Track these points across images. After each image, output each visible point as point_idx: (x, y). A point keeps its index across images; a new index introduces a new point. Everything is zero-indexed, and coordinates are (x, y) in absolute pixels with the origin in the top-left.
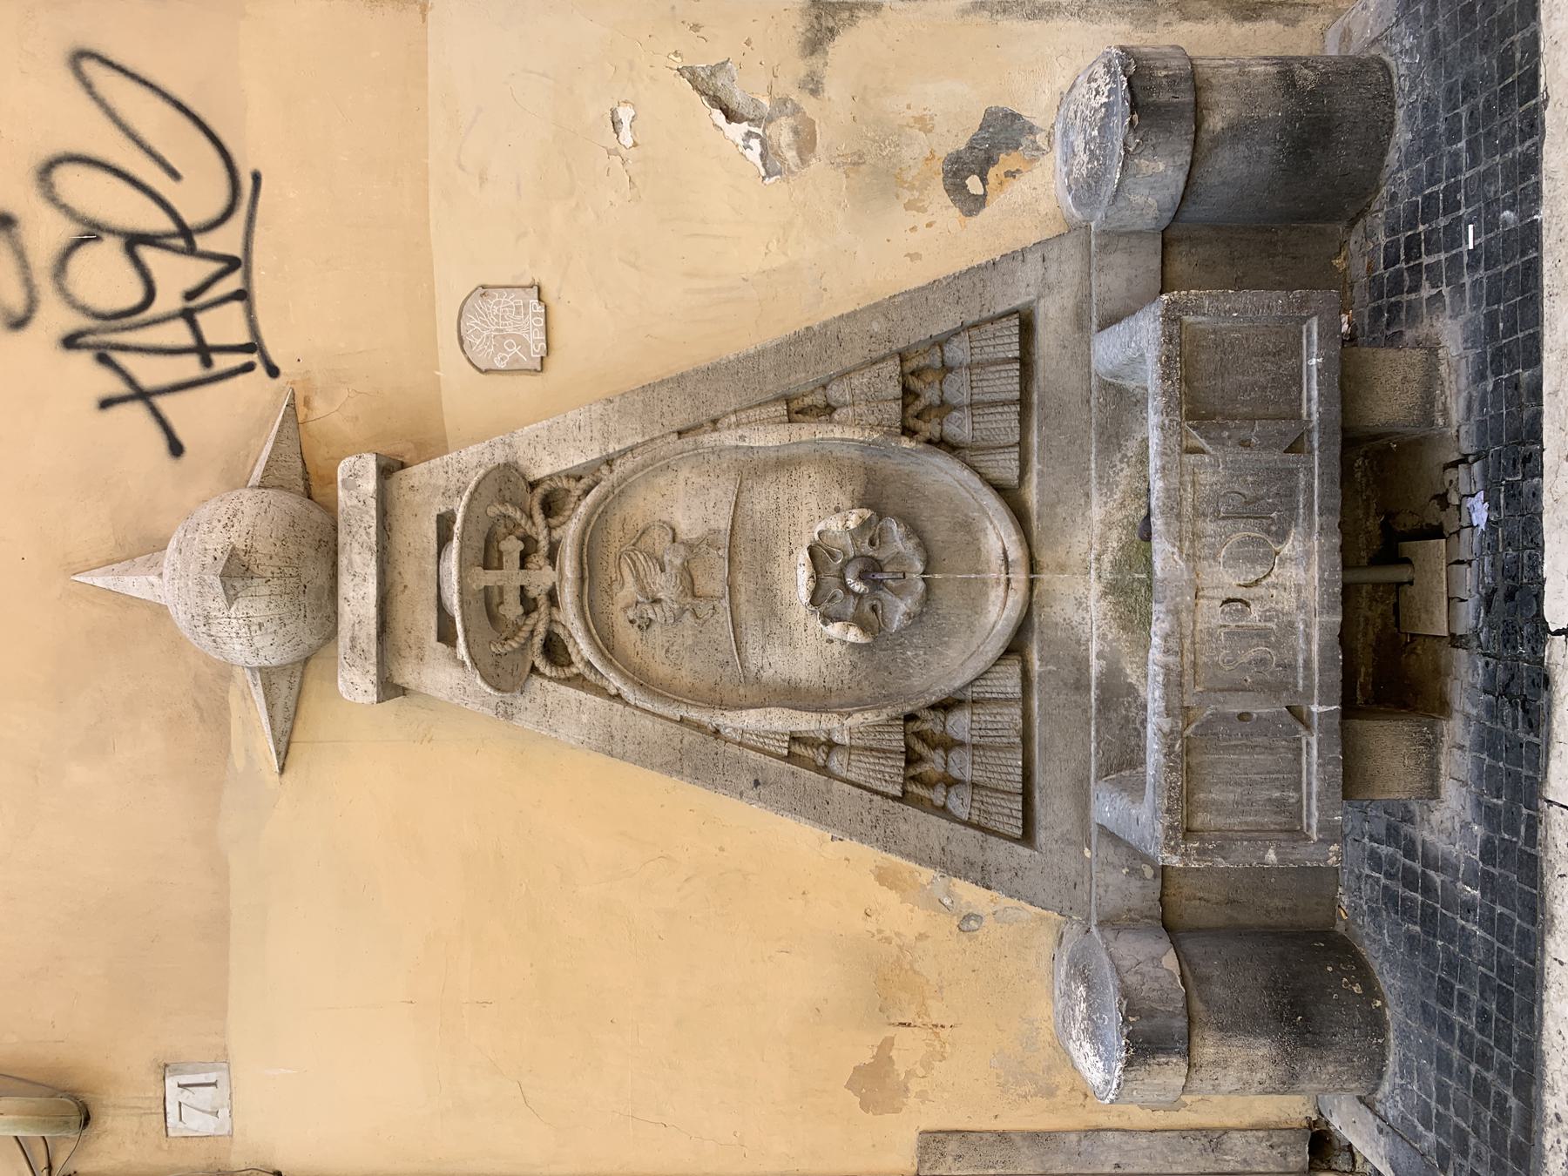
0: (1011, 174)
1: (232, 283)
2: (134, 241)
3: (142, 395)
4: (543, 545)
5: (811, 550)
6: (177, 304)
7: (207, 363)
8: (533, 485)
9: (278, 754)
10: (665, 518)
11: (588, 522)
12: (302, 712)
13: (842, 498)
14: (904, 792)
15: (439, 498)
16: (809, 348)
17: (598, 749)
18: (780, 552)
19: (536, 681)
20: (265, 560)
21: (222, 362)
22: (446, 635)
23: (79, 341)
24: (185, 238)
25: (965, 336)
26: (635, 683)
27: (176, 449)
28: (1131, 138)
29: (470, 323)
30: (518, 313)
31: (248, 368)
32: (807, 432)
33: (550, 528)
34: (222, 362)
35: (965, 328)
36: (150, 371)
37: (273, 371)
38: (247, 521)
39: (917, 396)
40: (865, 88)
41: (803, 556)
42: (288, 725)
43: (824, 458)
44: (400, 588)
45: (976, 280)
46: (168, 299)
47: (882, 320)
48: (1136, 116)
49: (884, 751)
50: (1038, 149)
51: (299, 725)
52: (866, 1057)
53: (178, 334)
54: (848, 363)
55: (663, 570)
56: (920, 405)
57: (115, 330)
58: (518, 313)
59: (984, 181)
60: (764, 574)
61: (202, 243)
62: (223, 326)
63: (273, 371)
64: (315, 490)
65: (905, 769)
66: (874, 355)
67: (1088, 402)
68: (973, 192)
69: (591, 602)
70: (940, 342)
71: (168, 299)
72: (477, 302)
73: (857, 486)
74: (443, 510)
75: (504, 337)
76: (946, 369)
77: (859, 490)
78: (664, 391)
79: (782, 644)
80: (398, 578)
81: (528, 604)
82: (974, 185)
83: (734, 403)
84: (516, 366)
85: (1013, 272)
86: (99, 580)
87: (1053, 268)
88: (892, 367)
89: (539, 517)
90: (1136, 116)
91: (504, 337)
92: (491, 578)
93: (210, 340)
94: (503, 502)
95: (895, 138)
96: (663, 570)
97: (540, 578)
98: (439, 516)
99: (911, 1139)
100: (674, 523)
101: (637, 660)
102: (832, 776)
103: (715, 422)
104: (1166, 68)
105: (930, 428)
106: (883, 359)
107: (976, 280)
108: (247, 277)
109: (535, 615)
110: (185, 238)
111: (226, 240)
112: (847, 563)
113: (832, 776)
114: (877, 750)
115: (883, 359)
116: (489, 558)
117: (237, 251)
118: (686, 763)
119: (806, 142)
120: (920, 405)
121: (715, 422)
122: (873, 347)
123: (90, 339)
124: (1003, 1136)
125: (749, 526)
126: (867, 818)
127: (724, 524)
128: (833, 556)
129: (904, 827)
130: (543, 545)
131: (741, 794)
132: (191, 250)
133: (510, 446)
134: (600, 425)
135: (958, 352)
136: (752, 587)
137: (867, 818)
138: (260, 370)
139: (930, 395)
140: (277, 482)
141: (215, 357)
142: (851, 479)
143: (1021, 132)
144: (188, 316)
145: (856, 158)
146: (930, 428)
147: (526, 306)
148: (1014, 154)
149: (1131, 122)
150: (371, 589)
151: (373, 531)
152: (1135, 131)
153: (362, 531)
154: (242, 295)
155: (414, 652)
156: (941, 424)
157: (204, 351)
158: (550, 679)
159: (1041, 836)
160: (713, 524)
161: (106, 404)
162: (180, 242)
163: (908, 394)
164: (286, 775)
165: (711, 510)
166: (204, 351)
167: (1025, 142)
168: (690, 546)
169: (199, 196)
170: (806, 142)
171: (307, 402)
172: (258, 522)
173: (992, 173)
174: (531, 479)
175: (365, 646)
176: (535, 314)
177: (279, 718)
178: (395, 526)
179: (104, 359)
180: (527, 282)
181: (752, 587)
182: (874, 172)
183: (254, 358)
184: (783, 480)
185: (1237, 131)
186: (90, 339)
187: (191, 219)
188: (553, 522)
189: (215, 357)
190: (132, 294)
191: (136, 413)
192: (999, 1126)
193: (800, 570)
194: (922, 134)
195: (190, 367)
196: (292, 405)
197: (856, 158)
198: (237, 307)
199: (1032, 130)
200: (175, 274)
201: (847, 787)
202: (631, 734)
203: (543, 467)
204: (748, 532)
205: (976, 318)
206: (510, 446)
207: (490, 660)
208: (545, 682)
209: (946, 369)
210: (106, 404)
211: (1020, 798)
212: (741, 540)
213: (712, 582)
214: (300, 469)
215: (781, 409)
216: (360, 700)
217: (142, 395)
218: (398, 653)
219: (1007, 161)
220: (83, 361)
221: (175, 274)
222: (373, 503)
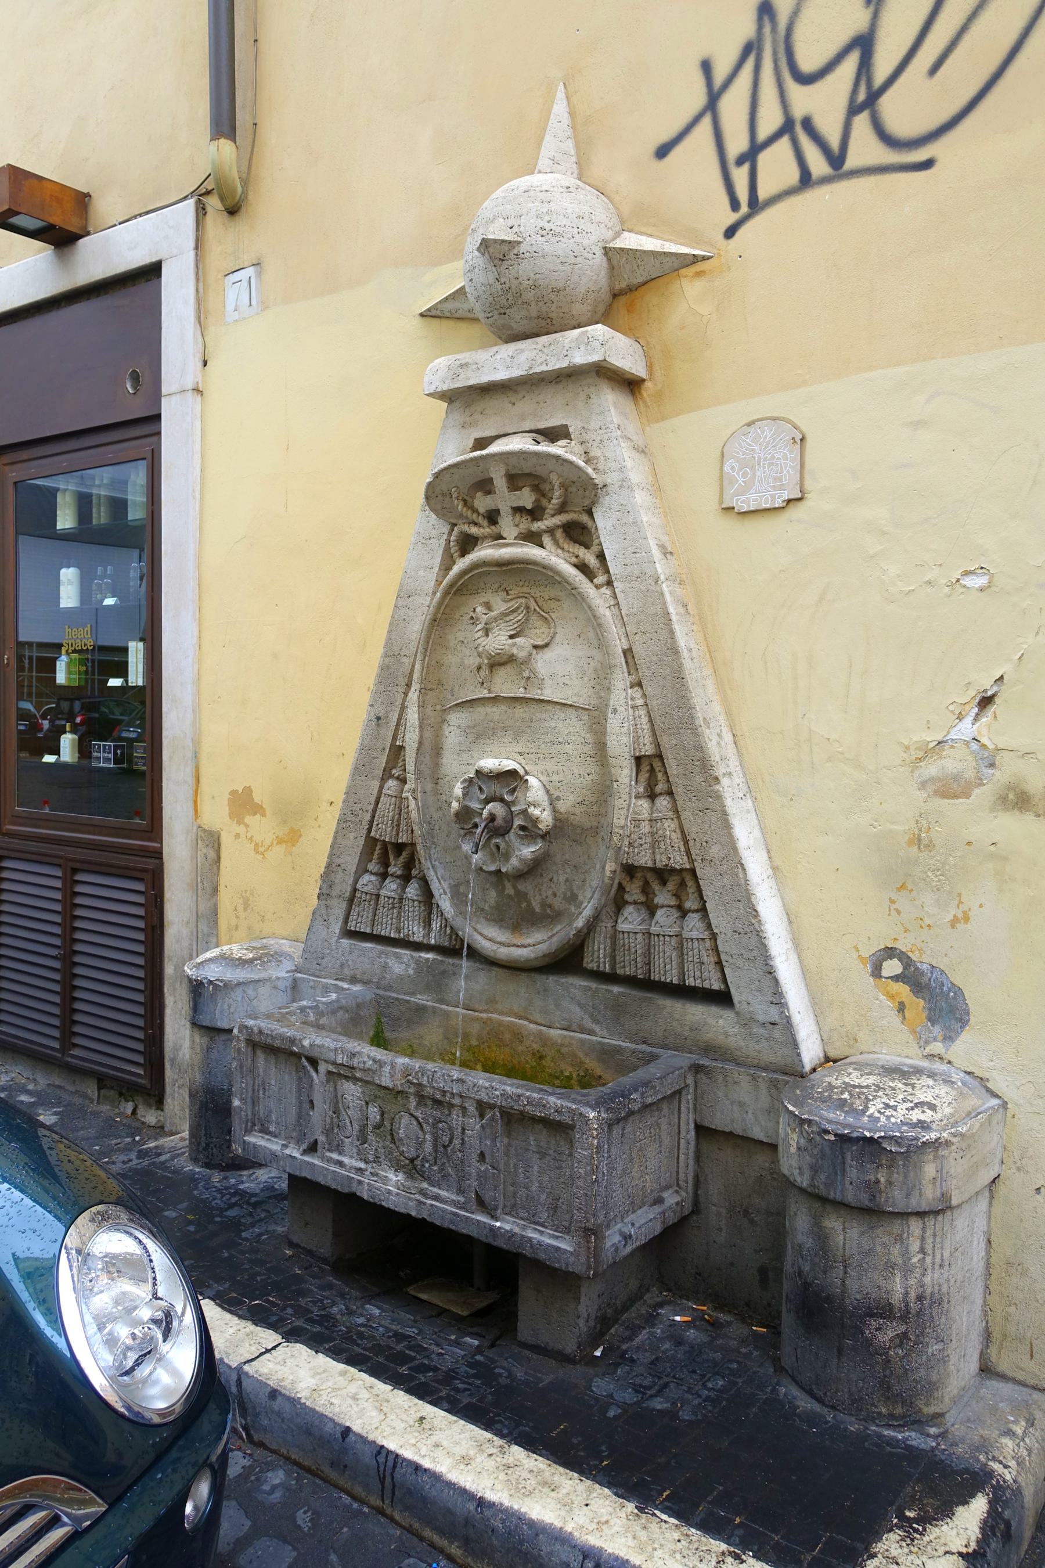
0: (901, 1008)
1: (818, 165)
2: (864, 44)
3: (713, 99)
4: (537, 526)
5: (512, 774)
6: (798, 113)
7: (740, 161)
8: (590, 513)
9: (429, 310)
10: (558, 638)
11: (544, 567)
12: (461, 325)
13: (569, 803)
14: (376, 840)
15: (580, 425)
16: (698, 779)
17: (401, 585)
18: (521, 744)
19: (446, 529)
20: (513, 272)
21: (740, 176)
22: (481, 443)
23: (766, 18)
24: (866, 101)
25: (706, 935)
26: (435, 614)
27: (663, 151)
28: (815, 1128)
29: (767, 431)
30: (775, 479)
31: (735, 205)
32: (624, 773)
33: (551, 531)
34: (740, 176)
35: (714, 937)
36: (734, 106)
37: (730, 232)
38: (549, 248)
39: (664, 883)
40: (1005, 859)
41: (509, 765)
42: (448, 315)
43: (604, 790)
44: (513, 399)
45: (755, 952)
46: (804, 100)
47: (721, 854)
48: (833, 1138)
49: (398, 826)
50: (927, 1042)
51: (451, 323)
52: (257, 798)
53: (770, 120)
54: (686, 816)
55: (511, 637)
56: (656, 886)
57: (775, 53)
58: (775, 479)
59: (896, 978)
60: (505, 729)
61: (862, 122)
62: (777, 167)
63: (730, 232)
64: (622, 300)
65: (390, 843)
66: (691, 843)
67: (645, 1043)
68: (885, 964)
69: (489, 573)
70: (703, 910)
71: (804, 100)
72: (788, 432)
73: (579, 816)
74: (571, 430)
75: (752, 468)
76: (683, 913)
77: (575, 820)
78: (664, 635)
79: (460, 743)
80: (520, 396)
81: (492, 516)
82: (892, 967)
83: (654, 703)
84: (725, 483)
85: (760, 990)
86: (560, 108)
87: (762, 1031)
88: (679, 860)
89: (557, 520)
90: (833, 1138)
91: (752, 468)
92: (500, 483)
93: (764, 158)
94: (562, 485)
95: (947, 888)
96: (511, 637)
97: (508, 526)
98: (566, 426)
99: (216, 827)
100: (552, 646)
101: (457, 616)
102: (383, 780)
103: (640, 684)
104: (890, 1183)
105: (634, 892)
106: (688, 852)
107: (755, 952)
108: (825, 180)
109: (485, 523)
110: (866, 101)
111: (865, 148)
112: (507, 804)
113: (383, 780)
114: (399, 820)
115: (688, 852)
116: (514, 481)
117: (850, 163)
118: (392, 660)
119: (951, 788)
120: (656, 886)
121: (640, 684)
122: (698, 843)
123: (767, 29)
124: (215, 891)
125: (544, 716)
126: (357, 807)
127: (548, 694)
128: (513, 791)
129: (352, 835)
130: (537, 526)
131: (372, 706)
132: (853, 110)
133: (621, 487)
134: (637, 572)
135: (693, 926)
136: (496, 718)
137: (357, 807)
138: (733, 217)
139: (663, 897)
140: (615, 262)
141: (746, 168)
142: (586, 813)
143: (947, 1028)
144: (787, 128)
145: (926, 842)
146: (634, 892)
147: (782, 488)
148: (925, 1015)
149: (827, 1132)
150: (501, 375)
151: (544, 368)
152: (819, 1134)
153: (544, 357)
154: (806, 180)
155: (468, 419)
156: (635, 903)
157: (750, 157)
158: (448, 541)
159: (346, 942)
160: (548, 682)
161: (706, 67)
162: (862, 97)
163: (663, 874)
164: (419, 318)
165: (561, 680)
166: (750, 157)
167: (937, 1030)
168: (526, 662)
169: (907, 108)
170: (951, 788)
171: (699, 274)
172: (549, 259)
173: (903, 990)
174: (594, 510)
175: (462, 376)
176: (773, 497)
177: (450, 306)
178: (560, 386)
179: (748, 49)
180: (808, 484)
181: (496, 718)
182: (910, 865)
183: (744, 209)
184: (586, 749)
185: (822, 1238)
186: (767, 29)
187: (887, 104)
188: (559, 534)
189: (746, 168)
190: (807, 63)
191: (698, 98)
192: (221, 888)
193: (497, 762)
194: (950, 917)
195: (737, 144)
196: (695, 259)
197: (926, 842)
198: (794, 175)
199: (949, 1039)
200: (826, 103)
201: (375, 792)
202: (410, 613)
203: (604, 523)
204: (539, 715)
205: (720, 949)
206: (621, 487)
207: (445, 488)
208: (445, 537)
209: (683, 913)
210: (706, 67)
211: (368, 931)
212: (533, 708)
213: (505, 684)
214: (636, 281)
215: (648, 749)
216: (426, 379)
217: (713, 99)
218: (468, 405)
219: (917, 1006)
220: (745, 28)
221: (826, 103)
222: (564, 364)
